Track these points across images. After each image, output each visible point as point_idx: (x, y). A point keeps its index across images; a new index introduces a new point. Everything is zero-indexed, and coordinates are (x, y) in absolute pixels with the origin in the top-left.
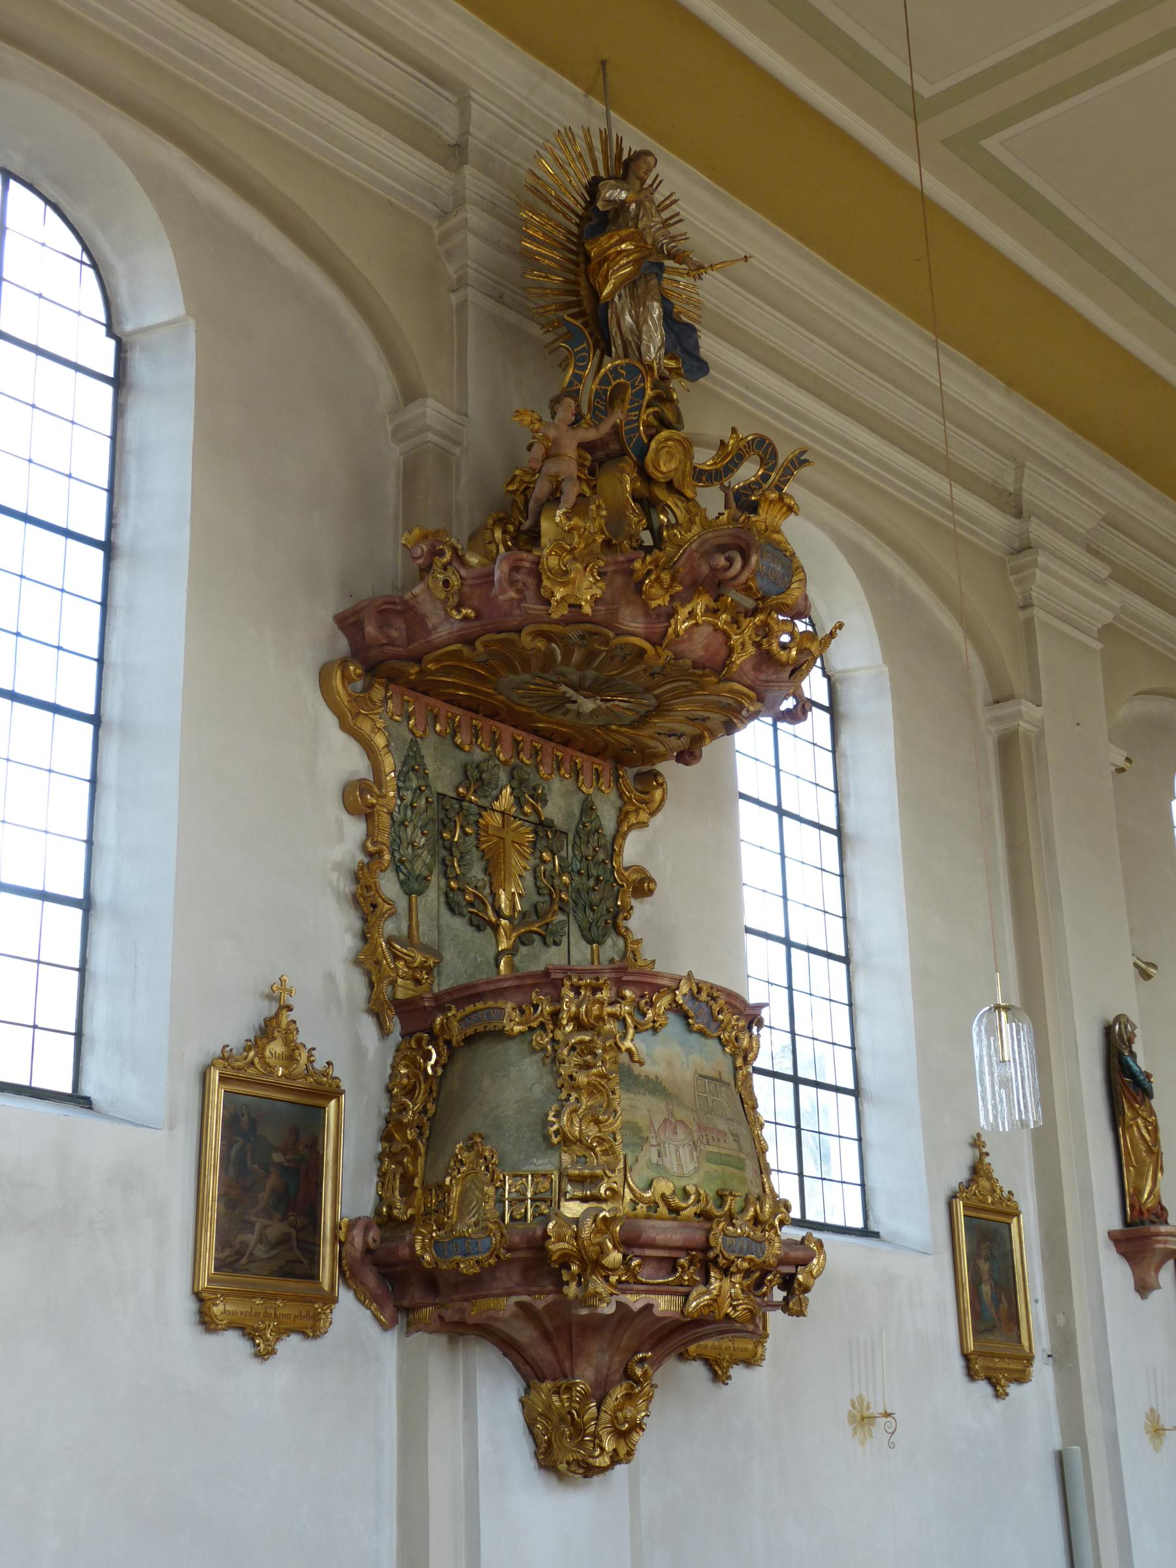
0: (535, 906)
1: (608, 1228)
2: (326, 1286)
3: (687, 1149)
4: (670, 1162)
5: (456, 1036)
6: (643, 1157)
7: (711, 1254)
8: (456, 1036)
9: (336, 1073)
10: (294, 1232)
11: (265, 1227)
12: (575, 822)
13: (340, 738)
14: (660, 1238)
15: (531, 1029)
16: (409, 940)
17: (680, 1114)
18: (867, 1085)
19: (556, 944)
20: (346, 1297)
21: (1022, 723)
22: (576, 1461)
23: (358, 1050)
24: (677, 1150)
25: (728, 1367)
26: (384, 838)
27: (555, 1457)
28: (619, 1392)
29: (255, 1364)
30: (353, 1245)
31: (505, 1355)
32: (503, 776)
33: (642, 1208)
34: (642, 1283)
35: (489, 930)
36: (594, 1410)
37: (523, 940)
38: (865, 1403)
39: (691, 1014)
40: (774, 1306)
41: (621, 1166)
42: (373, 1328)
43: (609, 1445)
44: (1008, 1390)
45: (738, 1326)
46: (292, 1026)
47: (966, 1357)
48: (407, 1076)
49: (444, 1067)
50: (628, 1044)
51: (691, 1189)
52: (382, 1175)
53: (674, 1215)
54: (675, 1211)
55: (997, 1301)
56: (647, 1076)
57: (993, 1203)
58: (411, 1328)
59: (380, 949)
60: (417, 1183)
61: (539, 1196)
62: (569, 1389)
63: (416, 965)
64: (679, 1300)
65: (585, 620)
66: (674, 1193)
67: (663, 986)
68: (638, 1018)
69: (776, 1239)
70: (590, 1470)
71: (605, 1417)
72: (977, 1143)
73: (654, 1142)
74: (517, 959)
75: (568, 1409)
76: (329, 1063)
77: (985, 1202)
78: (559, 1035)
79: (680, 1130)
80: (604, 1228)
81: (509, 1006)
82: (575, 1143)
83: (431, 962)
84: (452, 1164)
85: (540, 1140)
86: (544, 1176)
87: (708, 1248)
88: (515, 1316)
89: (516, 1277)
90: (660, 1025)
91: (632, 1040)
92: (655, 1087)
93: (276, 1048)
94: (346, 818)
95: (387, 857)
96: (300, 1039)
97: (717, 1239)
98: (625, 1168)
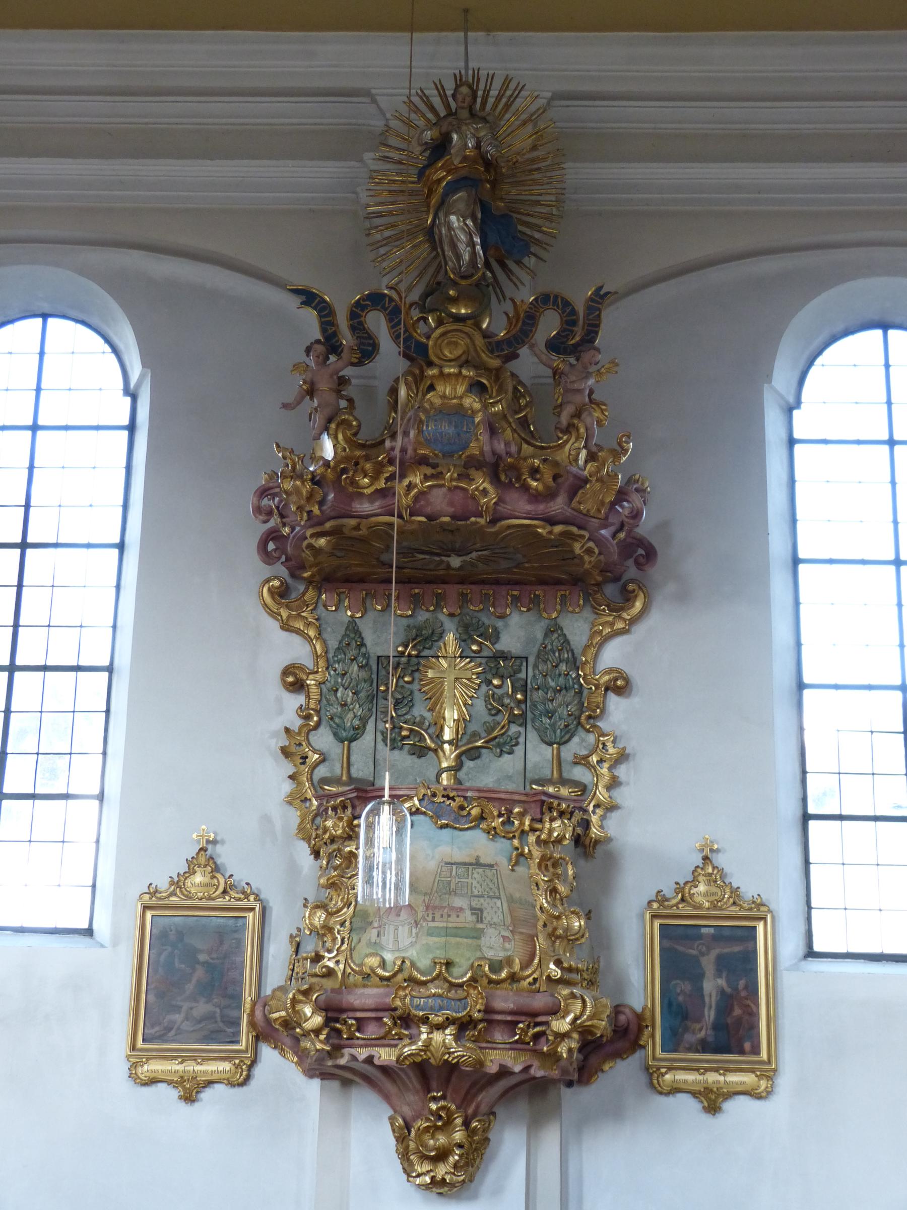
3: (407, 928)
6: (365, 938)
10: (218, 1010)
11: (191, 1008)
12: (537, 646)
19: (511, 752)
23: (293, 868)
37: (473, 754)
73: (376, 925)
74: (461, 775)
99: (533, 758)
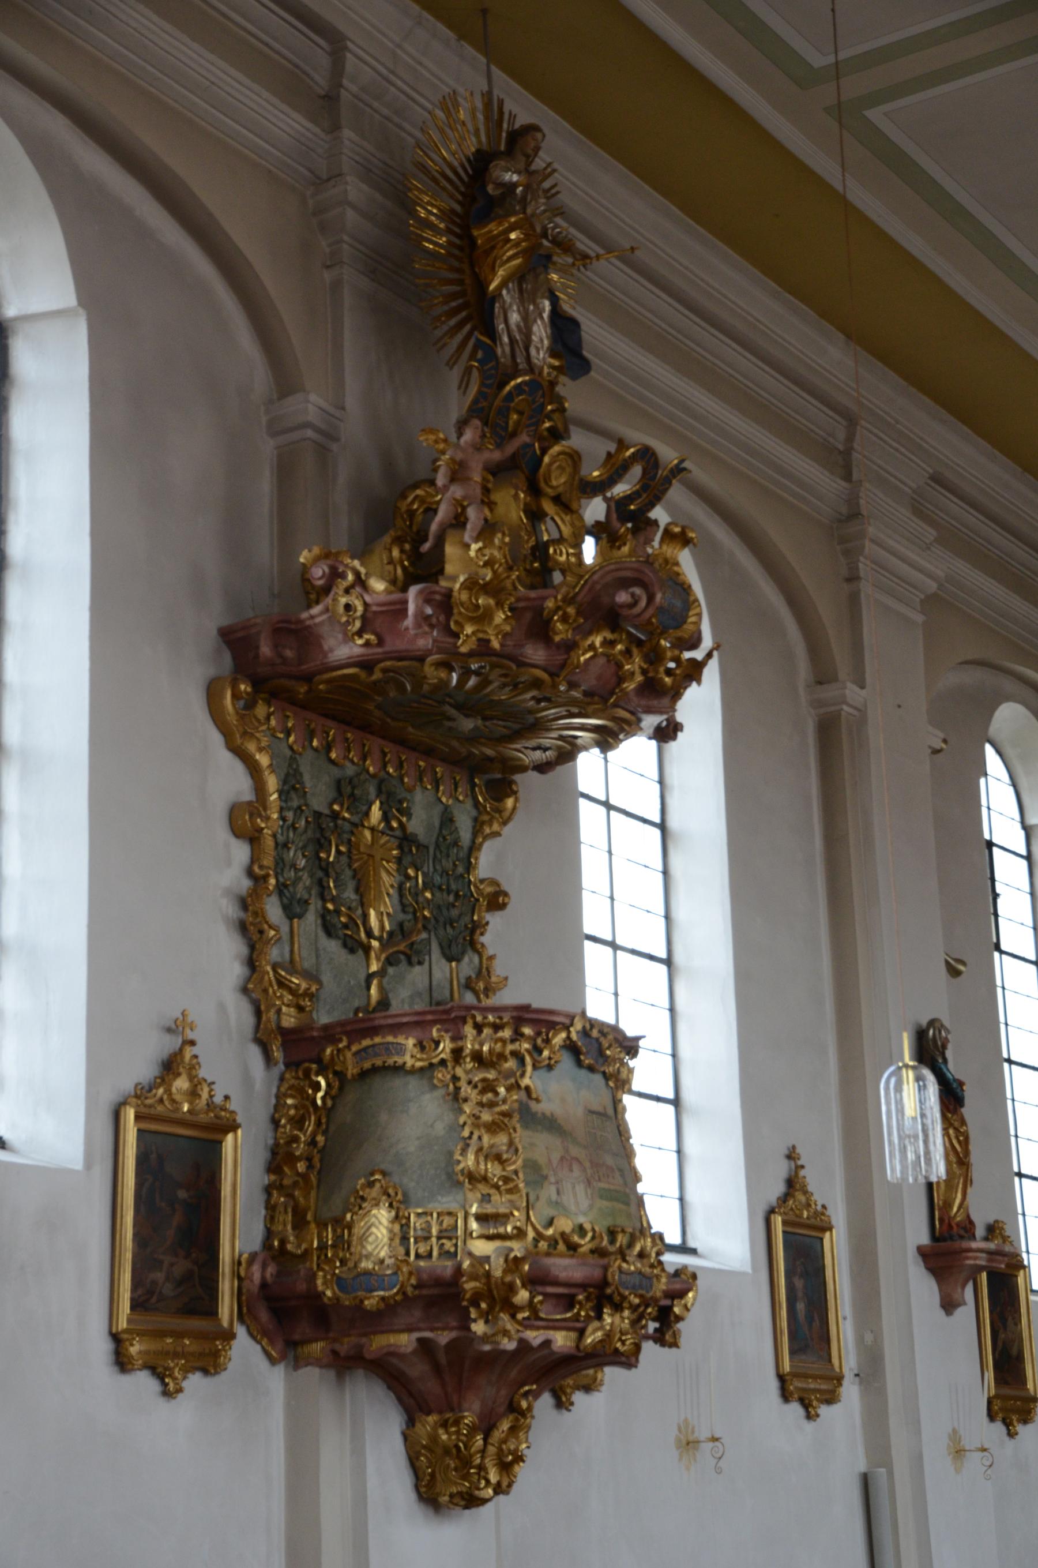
0: (401, 925)
1: (517, 1268)
2: (225, 1323)
4: (567, 1199)
5: (352, 1071)
7: (609, 1291)
8: (352, 1071)
9: (232, 1106)
11: (172, 1265)
12: (435, 835)
13: (226, 758)
14: (563, 1275)
15: (431, 1065)
16: (292, 967)
17: (575, 1151)
18: (688, 1096)
19: (420, 963)
20: (241, 1331)
21: (845, 707)
22: (460, 1494)
23: (247, 1080)
24: (574, 1187)
25: (571, 1394)
26: (268, 861)
27: (438, 1490)
28: (505, 1425)
29: (162, 1401)
30: (252, 1281)
31: (389, 1388)
32: (372, 791)
33: (543, 1245)
34: (542, 1319)
35: (360, 952)
36: (480, 1443)
38: (690, 1427)
39: (584, 1050)
40: (647, 1337)
41: (524, 1204)
42: (263, 1363)
43: (493, 1477)
44: (819, 1411)
45: (623, 1359)
46: (195, 1061)
47: (781, 1378)
48: (296, 1107)
49: (333, 1098)
50: (526, 1081)
51: (587, 1226)
52: (271, 1208)
53: (572, 1252)
54: (573, 1247)
55: (810, 1320)
56: (543, 1114)
57: (808, 1218)
58: (298, 1364)
59: (266, 978)
60: (309, 1217)
61: (445, 1234)
62: (457, 1422)
63: (301, 992)
64: (573, 1335)
65: (494, 653)
66: (573, 1231)
67: (558, 1023)
68: (535, 1055)
69: (663, 1274)
70: (471, 1501)
71: (491, 1450)
72: (791, 1155)
73: (552, 1179)
74: (385, 980)
75: (455, 1442)
76: (227, 1098)
77: (801, 1216)
78: (459, 1071)
79: (575, 1167)
80: (514, 1267)
81: (411, 1042)
82: (480, 1182)
83: (313, 989)
84: (352, 1200)
85: (444, 1177)
86: (450, 1214)
87: (605, 1283)
88: (414, 1352)
89: (417, 1313)
90: (556, 1062)
91: (531, 1078)
92: (550, 1124)
93: (181, 1084)
94: (234, 842)
95: (272, 881)
96: (202, 1073)
97: (613, 1276)
98: (528, 1207)
99: (437, 975)
